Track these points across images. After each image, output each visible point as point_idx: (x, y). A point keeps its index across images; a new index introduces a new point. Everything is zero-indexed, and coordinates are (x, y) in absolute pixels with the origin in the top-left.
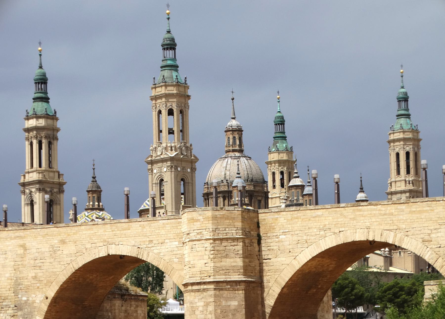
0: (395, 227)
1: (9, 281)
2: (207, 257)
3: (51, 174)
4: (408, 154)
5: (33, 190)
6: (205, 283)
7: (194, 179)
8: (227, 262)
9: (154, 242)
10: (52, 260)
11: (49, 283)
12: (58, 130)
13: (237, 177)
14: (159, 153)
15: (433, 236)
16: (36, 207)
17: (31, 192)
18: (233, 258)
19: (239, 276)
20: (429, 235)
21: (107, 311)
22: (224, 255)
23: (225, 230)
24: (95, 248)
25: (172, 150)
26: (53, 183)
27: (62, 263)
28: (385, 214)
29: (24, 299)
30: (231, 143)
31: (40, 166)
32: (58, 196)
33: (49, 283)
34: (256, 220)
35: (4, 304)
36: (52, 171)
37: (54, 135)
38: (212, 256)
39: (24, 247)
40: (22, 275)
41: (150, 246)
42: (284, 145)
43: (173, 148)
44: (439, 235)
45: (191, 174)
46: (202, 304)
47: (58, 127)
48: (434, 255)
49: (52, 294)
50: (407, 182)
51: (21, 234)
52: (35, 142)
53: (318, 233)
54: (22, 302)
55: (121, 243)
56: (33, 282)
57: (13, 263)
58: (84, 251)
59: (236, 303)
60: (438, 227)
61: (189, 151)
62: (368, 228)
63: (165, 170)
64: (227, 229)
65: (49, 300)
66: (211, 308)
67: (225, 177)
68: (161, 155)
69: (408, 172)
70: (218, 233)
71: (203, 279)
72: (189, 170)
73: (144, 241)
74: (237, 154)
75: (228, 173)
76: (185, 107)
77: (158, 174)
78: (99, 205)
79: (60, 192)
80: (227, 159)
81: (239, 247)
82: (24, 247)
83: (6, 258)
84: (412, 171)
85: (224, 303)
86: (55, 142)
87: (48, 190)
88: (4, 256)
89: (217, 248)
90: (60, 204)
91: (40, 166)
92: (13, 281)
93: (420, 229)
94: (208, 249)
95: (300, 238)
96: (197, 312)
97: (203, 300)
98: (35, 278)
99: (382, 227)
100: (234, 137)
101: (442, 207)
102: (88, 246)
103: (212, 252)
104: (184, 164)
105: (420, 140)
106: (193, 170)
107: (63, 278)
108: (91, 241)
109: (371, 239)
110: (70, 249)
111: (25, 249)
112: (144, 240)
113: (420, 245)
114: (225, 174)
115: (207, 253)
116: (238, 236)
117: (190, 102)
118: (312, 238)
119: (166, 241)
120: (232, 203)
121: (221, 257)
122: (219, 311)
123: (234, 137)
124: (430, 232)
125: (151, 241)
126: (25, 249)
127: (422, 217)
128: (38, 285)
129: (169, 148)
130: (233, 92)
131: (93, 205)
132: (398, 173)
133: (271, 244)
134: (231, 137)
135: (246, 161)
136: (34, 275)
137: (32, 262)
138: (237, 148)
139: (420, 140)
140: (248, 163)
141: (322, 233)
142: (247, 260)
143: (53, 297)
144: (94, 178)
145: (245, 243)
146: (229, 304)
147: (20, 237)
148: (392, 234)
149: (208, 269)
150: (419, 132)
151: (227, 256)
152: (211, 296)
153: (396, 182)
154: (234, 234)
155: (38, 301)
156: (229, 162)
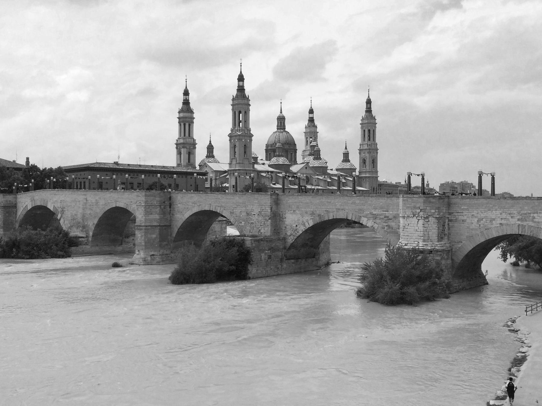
0: (220, 205)
2: (142, 214)
3: (190, 140)
4: (369, 131)
5: (181, 147)
6: (141, 226)
7: (251, 145)
8: (151, 217)
9: (133, 202)
10: (96, 207)
11: (95, 217)
12: (194, 118)
13: (278, 143)
14: (234, 133)
15: (234, 210)
16: (182, 155)
17: (180, 148)
18: (154, 215)
19: (157, 223)
20: (233, 210)
21: (132, 228)
22: (150, 213)
23: (151, 202)
25: (240, 131)
26: (191, 144)
27: (100, 208)
28: (217, 198)
29: (86, 223)
30: (279, 125)
31: (185, 136)
32: (193, 150)
33: (95, 217)
34: (169, 196)
35: (79, 225)
36: (190, 138)
37: (191, 120)
38: (144, 214)
40: (85, 213)
41: (131, 204)
42: (313, 124)
43: (241, 130)
44: (236, 210)
45: (249, 143)
46: (139, 235)
47: (194, 117)
48: (234, 220)
49: (96, 222)
50: (369, 145)
51: (86, 193)
52: (182, 124)
53: (192, 205)
54: (85, 225)
56: (89, 216)
57: (82, 207)
58: (108, 204)
59: (155, 236)
60: (236, 206)
61: (249, 132)
62: (210, 204)
63: (237, 140)
64: (152, 201)
65: (95, 224)
66: (143, 238)
67: (275, 142)
68: (235, 133)
69: (369, 140)
70: (148, 203)
71: (141, 224)
72: (248, 141)
73: (129, 202)
74: (282, 131)
75: (276, 140)
76: (247, 110)
77: (233, 143)
78: (212, 155)
79: (194, 149)
80: (276, 133)
81: (158, 210)
83: (80, 204)
84: (372, 139)
85: (149, 236)
86: (192, 124)
87: (188, 147)
89: (147, 210)
90: (194, 154)
91: (185, 136)
93: (229, 207)
94: (143, 210)
95: (185, 206)
96: (138, 239)
97: (140, 234)
98: (90, 214)
99: (216, 205)
100: (281, 122)
101: (238, 197)
103: (145, 212)
104: (246, 138)
105: (377, 123)
106: (251, 140)
107: (100, 215)
109: (211, 210)
110: (102, 202)
111: (87, 200)
112: (129, 201)
113: (229, 214)
114: (275, 140)
115: (143, 212)
116: (157, 205)
117: (250, 107)
118: (190, 207)
120: (275, 155)
121: (149, 214)
122: (146, 239)
123: (281, 122)
124: (233, 209)
125: (131, 202)
126: (87, 200)
127: (231, 201)
129: (239, 130)
130: (281, 100)
131: (210, 155)
132: (364, 140)
133: (175, 208)
134: (279, 122)
135: (286, 134)
137: (89, 206)
138: (282, 127)
139: (377, 123)
140: (287, 135)
141: (193, 205)
142: (162, 216)
143: (96, 224)
144: (210, 141)
145: (161, 208)
146: (152, 236)
147: (85, 195)
148: (219, 208)
149: (143, 219)
150: (376, 120)
151: (151, 214)
152: (143, 232)
153: (363, 144)
154: (155, 203)
155: (91, 225)
156: (277, 134)
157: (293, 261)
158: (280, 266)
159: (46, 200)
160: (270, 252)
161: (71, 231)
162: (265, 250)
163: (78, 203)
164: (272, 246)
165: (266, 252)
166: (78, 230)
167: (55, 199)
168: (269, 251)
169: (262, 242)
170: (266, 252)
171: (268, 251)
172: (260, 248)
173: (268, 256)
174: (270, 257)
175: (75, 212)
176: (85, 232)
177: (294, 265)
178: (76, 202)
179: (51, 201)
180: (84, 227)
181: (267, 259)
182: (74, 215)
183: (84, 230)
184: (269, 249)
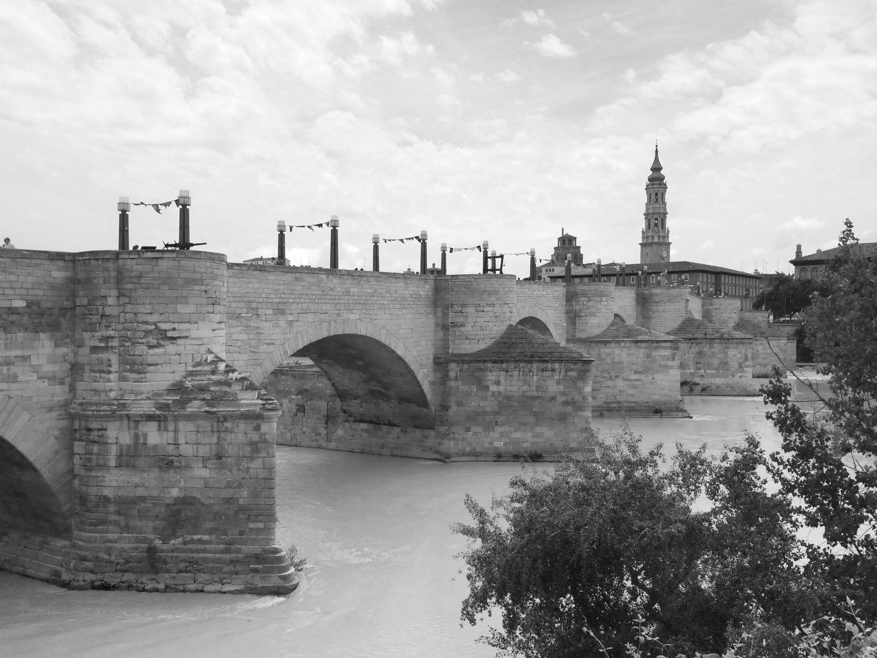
157: (364, 426)
158: (323, 431)
160: (303, 398)
162: (289, 393)
164: (306, 387)
165: (293, 397)
168: (299, 397)
169: (283, 377)
170: (293, 397)
171: (297, 395)
172: (279, 389)
173: (296, 405)
174: (301, 409)
177: (365, 435)
181: (294, 411)
184: (299, 393)
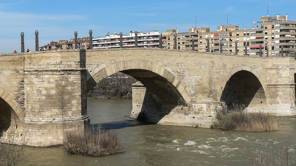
1: (207, 79)
24: (239, 66)
29: (213, 88)
35: (205, 90)
39: (212, 62)
55: (246, 65)
56: (217, 80)
82: (212, 62)
88: (205, 66)
92: (209, 79)
98: (217, 78)
102: (236, 65)
108: (237, 63)
110: (229, 66)
119: (259, 66)
128: (218, 82)
136: (217, 77)
147: (210, 57)
159: (150, 62)
161: (196, 98)
163: (203, 66)
166: (204, 96)
167: (166, 62)
175: (200, 76)
176: (212, 98)
178: (201, 65)
179: (160, 64)
180: (211, 92)
182: (198, 80)
183: (211, 95)
